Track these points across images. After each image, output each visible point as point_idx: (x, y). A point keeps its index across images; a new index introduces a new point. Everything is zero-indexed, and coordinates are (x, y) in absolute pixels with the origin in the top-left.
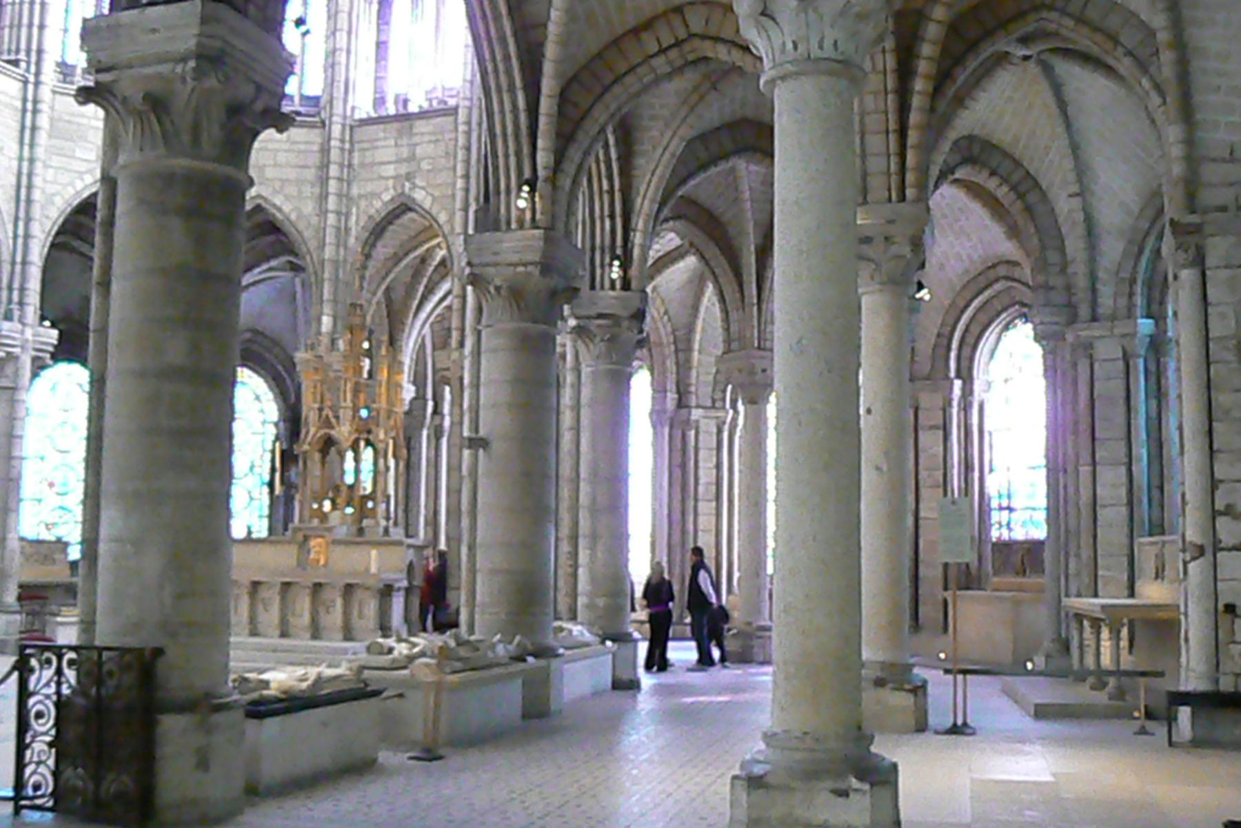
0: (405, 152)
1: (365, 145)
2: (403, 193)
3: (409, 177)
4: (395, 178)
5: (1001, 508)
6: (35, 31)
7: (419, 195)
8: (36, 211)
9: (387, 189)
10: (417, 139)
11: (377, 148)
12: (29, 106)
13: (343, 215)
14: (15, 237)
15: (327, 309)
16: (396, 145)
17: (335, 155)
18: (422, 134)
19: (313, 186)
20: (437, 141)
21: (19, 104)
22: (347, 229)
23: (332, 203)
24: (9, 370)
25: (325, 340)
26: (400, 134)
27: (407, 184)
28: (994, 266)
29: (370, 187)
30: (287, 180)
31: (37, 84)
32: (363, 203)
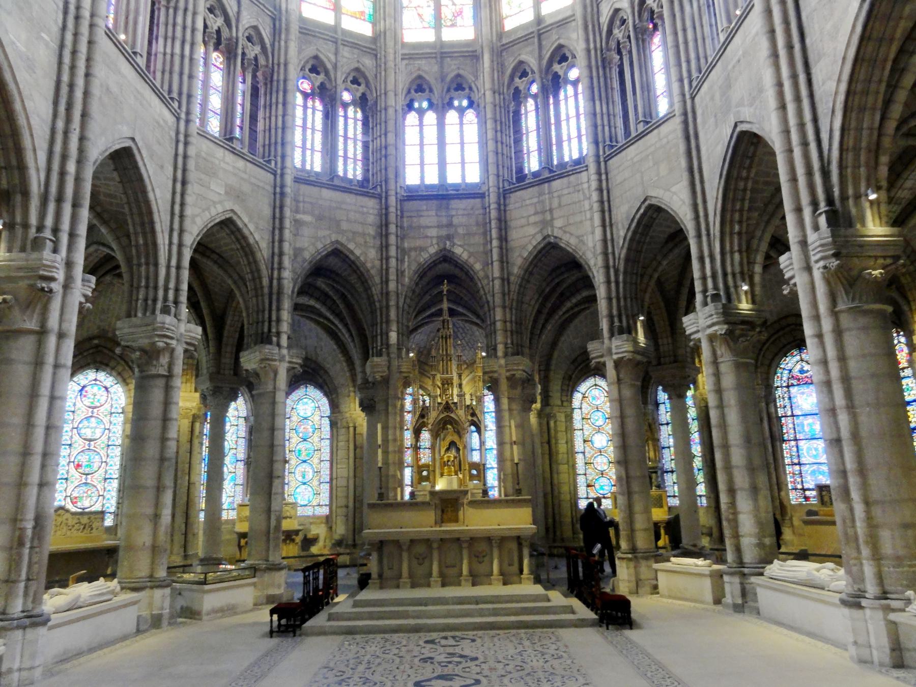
0: (444, 221)
1: (412, 214)
2: (445, 249)
3: (449, 237)
4: (438, 237)
5: (794, 464)
6: (185, 78)
7: (458, 251)
8: (187, 224)
9: (432, 245)
10: (454, 213)
11: (422, 216)
12: (182, 138)
13: (399, 260)
14: (170, 244)
15: (394, 327)
16: (437, 215)
17: (392, 218)
18: (457, 209)
19: (374, 238)
20: (468, 214)
21: (173, 134)
22: (403, 272)
23: (393, 252)
24: (164, 360)
25: (394, 350)
26: (439, 208)
27: (448, 243)
28: (786, 317)
29: (419, 243)
30: (358, 233)
31: (188, 121)
32: (413, 254)
